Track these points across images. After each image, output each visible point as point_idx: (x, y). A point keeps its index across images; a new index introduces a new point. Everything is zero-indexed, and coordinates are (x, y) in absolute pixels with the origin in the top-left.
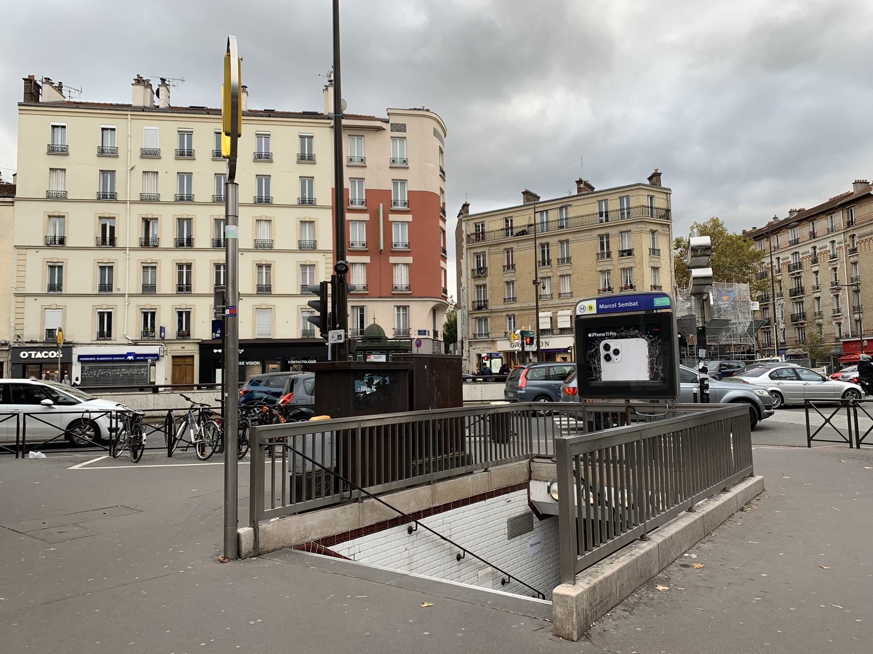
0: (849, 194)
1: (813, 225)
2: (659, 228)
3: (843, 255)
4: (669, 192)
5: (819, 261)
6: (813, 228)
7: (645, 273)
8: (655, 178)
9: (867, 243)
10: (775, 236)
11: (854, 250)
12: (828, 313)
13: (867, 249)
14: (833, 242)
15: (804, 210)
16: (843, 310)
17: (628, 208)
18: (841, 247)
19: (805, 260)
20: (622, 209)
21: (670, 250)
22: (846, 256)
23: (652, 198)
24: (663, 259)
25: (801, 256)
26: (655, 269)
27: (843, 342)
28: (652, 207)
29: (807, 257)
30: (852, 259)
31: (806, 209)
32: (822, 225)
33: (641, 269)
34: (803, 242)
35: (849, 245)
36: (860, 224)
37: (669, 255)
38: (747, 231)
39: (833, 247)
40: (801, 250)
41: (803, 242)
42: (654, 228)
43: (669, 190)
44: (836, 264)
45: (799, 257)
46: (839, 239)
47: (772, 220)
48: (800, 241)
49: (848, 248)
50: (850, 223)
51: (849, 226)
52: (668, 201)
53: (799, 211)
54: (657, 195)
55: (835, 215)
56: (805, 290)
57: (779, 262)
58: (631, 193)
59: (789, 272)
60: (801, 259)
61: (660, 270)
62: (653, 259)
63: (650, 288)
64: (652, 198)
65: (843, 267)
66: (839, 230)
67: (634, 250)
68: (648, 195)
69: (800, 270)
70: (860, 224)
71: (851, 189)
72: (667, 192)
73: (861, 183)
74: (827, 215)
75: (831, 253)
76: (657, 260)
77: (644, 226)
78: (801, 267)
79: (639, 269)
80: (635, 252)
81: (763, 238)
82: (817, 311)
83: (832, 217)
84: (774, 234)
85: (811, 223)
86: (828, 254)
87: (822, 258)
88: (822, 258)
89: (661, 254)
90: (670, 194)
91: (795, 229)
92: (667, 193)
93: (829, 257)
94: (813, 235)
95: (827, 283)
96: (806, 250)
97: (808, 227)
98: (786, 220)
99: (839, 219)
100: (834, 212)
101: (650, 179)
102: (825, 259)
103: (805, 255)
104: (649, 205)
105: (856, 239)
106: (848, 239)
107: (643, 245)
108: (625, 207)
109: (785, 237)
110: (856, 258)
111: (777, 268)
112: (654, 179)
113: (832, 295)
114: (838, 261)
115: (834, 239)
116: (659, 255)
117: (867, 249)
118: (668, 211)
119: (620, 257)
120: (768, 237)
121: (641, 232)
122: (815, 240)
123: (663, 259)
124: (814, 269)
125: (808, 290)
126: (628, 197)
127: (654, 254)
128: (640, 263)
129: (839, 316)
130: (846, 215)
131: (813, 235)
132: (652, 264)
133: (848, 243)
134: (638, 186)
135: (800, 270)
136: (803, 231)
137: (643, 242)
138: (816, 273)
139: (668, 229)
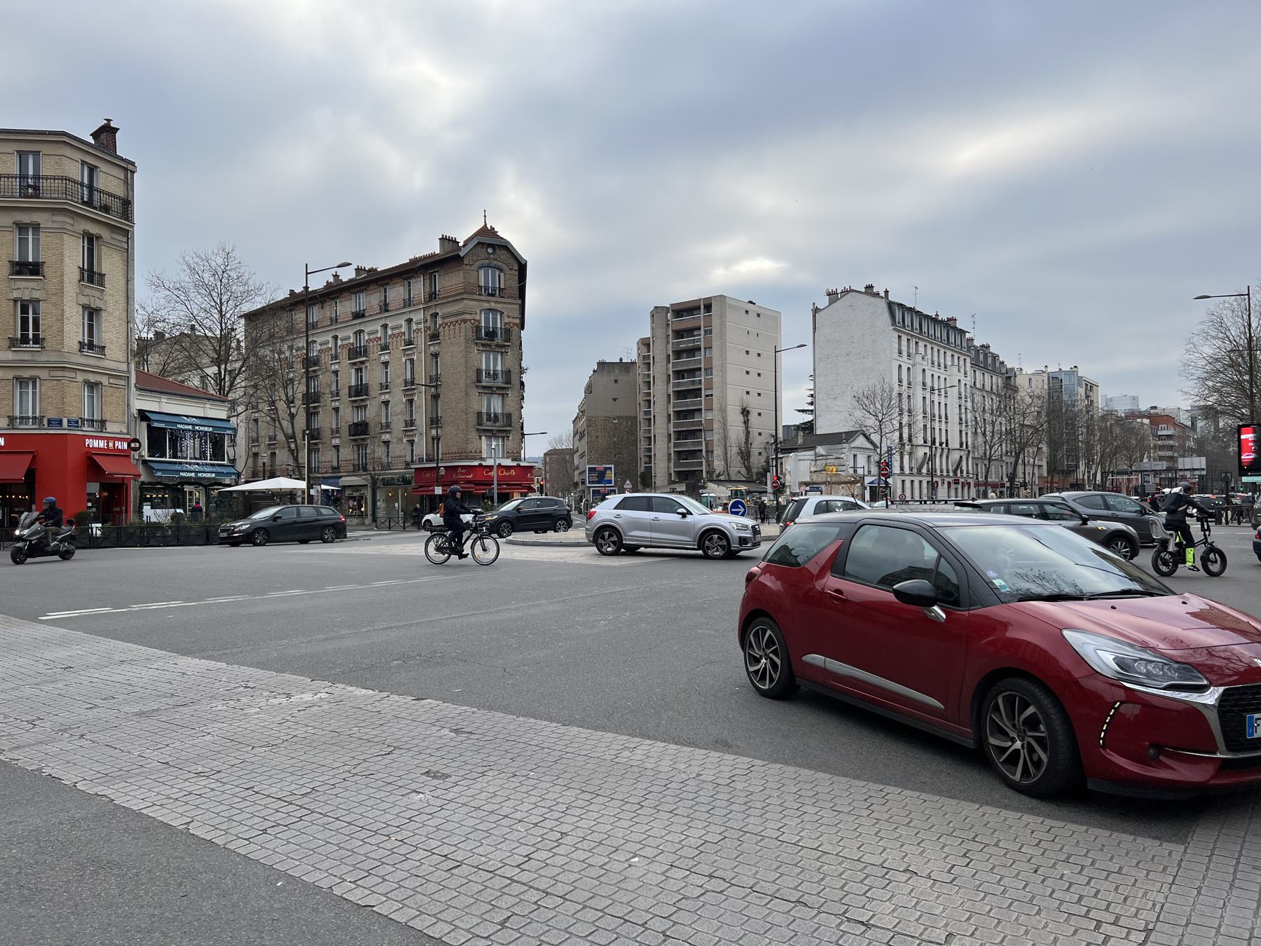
0: (433, 255)
1: (385, 292)
2: (106, 234)
3: (421, 340)
4: (130, 167)
5: (391, 348)
6: (385, 296)
7: (67, 314)
8: (106, 133)
9: (452, 327)
10: (333, 302)
11: (435, 336)
12: (398, 425)
13: (452, 336)
14: (409, 321)
15: (376, 270)
16: (417, 423)
17: (37, 177)
18: (419, 330)
19: (371, 344)
20: (23, 177)
21: (128, 281)
22: (425, 343)
23: (92, 169)
24: (112, 295)
25: (367, 338)
26: (92, 313)
27: (415, 469)
28: (91, 188)
29: (375, 339)
30: (432, 349)
31: (379, 270)
32: (396, 293)
33: (59, 306)
34: (370, 315)
35: (429, 328)
36: (445, 298)
37: (125, 289)
38: (297, 291)
39: (410, 328)
40: (368, 329)
41: (370, 315)
42: (94, 229)
43: (133, 164)
44: (411, 354)
45: (364, 338)
46: (418, 316)
47: (331, 280)
48: (366, 314)
49: (428, 332)
50: (432, 296)
51: (430, 300)
52: (129, 185)
53: (371, 270)
54: (103, 167)
55: (414, 280)
56: (370, 389)
57: (336, 344)
58: (44, 149)
59: (349, 359)
60: (367, 341)
61: (104, 314)
62: (87, 291)
63: (77, 347)
64: (92, 169)
65: (420, 358)
66: (418, 304)
67: (45, 265)
68: (83, 163)
69: (365, 359)
70: (445, 298)
71: (436, 248)
72: (128, 169)
73: (449, 240)
74: (404, 279)
75: (407, 337)
76: (98, 294)
77: (70, 221)
78: (366, 353)
79: (55, 305)
80: (47, 270)
81: (315, 304)
82: (384, 421)
83: (409, 283)
84: (331, 299)
85: (382, 289)
86: (403, 337)
87: (395, 342)
88: (395, 342)
89: (107, 283)
90: (133, 172)
91: (361, 295)
92: (126, 169)
93: (403, 342)
94: (385, 308)
95: (399, 381)
96: (372, 328)
97: (378, 294)
98: (350, 281)
99: (419, 287)
100: (413, 276)
101: (95, 135)
102: (399, 344)
103: (372, 336)
104: (86, 182)
105: (439, 321)
106: (429, 318)
107: (67, 260)
108: (31, 172)
109: (346, 307)
110: (437, 348)
111: (333, 352)
112: (103, 136)
113: (404, 400)
114: (415, 350)
115: (412, 316)
116: (102, 285)
117: (452, 336)
118: (127, 205)
119: (13, 275)
120: (322, 303)
121: (63, 230)
122: (387, 314)
123: (112, 295)
124: (386, 358)
125: (374, 390)
126: (36, 153)
127: (91, 280)
128: (56, 294)
129: (412, 430)
130: (428, 282)
131: (385, 308)
132: (85, 301)
133: (428, 324)
134: (62, 139)
135: (365, 359)
136: (370, 301)
137: (67, 253)
138: (386, 364)
139: (125, 239)
